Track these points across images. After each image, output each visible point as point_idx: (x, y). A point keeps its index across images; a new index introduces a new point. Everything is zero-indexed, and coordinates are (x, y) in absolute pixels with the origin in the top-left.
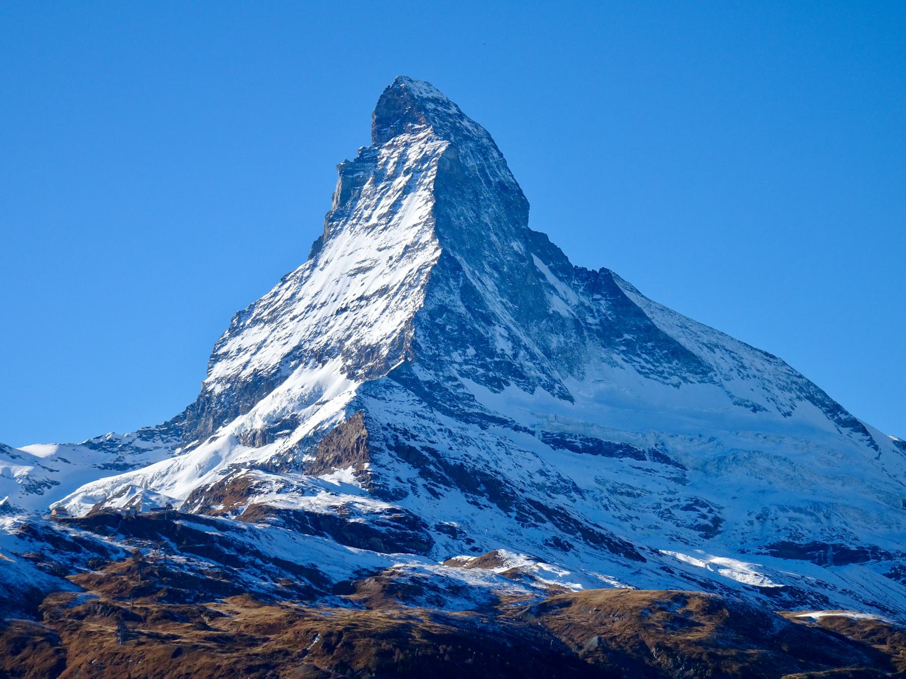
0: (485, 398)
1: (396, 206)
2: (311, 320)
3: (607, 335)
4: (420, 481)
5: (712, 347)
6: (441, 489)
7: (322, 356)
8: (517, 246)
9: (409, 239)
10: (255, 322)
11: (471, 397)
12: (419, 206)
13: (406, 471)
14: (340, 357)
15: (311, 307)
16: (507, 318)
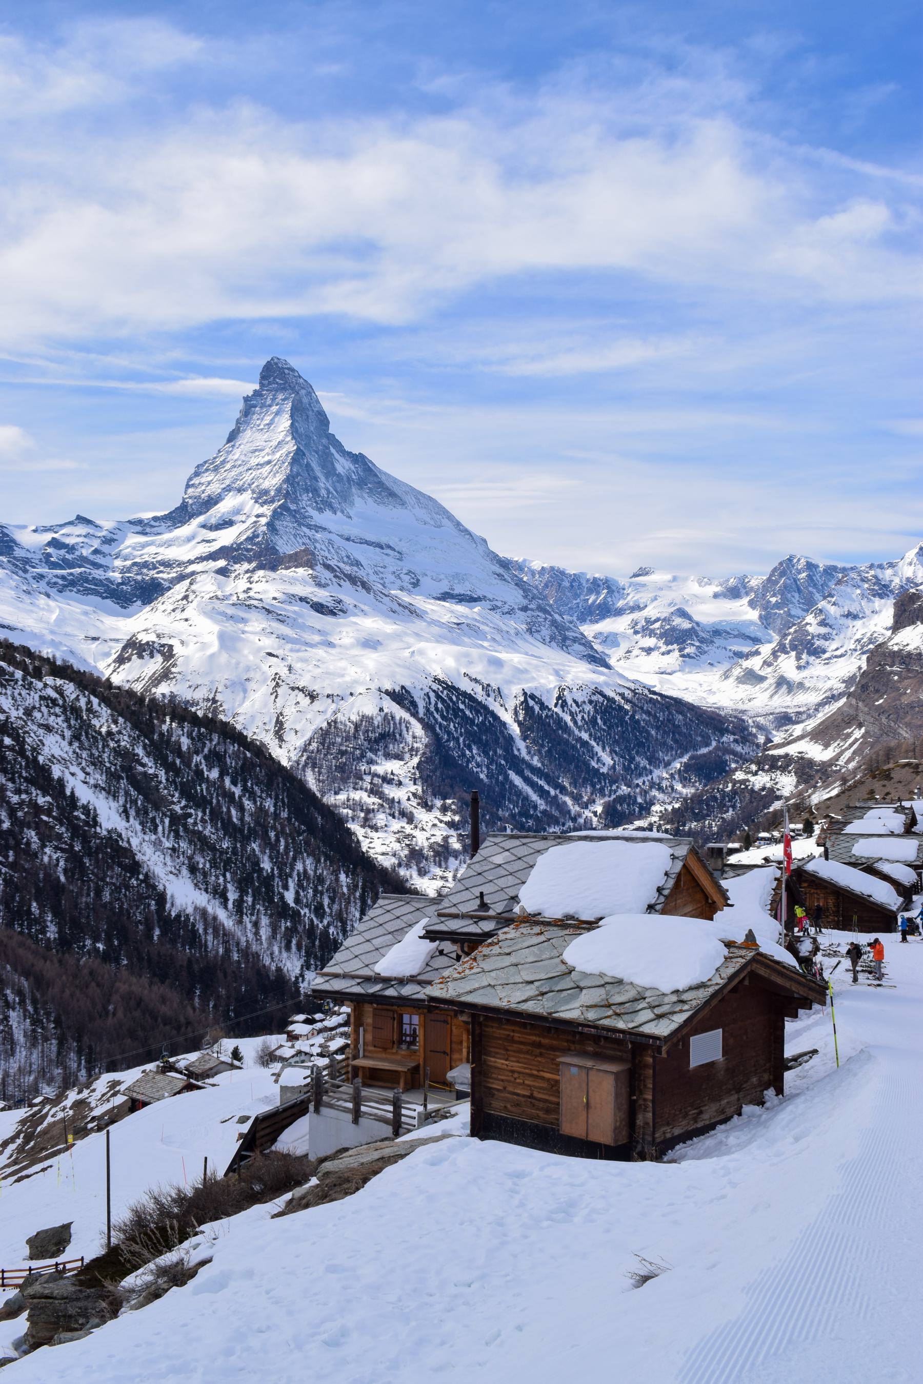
0: (318, 518)
1: (272, 421)
2: (233, 473)
3: (361, 484)
4: (334, 580)
5: (406, 493)
6: (342, 582)
7: (240, 490)
8: (324, 441)
9: (281, 438)
10: (207, 470)
11: (311, 517)
12: (285, 422)
13: (329, 575)
14: (250, 492)
15: (234, 466)
16: (323, 479)
